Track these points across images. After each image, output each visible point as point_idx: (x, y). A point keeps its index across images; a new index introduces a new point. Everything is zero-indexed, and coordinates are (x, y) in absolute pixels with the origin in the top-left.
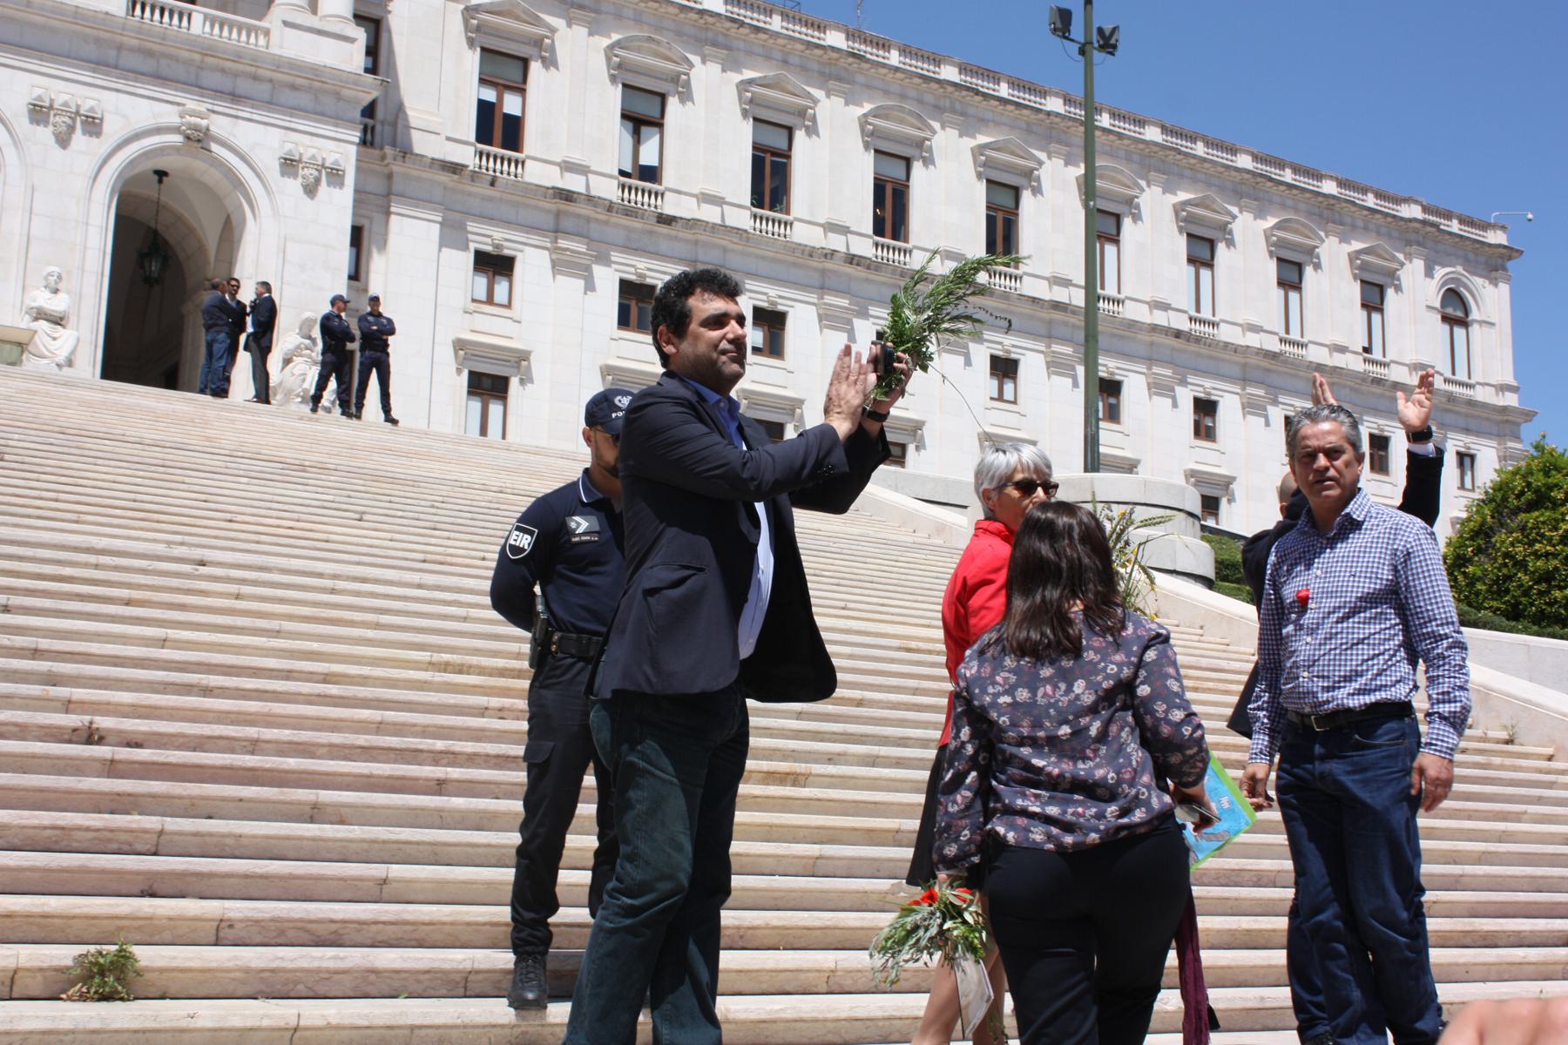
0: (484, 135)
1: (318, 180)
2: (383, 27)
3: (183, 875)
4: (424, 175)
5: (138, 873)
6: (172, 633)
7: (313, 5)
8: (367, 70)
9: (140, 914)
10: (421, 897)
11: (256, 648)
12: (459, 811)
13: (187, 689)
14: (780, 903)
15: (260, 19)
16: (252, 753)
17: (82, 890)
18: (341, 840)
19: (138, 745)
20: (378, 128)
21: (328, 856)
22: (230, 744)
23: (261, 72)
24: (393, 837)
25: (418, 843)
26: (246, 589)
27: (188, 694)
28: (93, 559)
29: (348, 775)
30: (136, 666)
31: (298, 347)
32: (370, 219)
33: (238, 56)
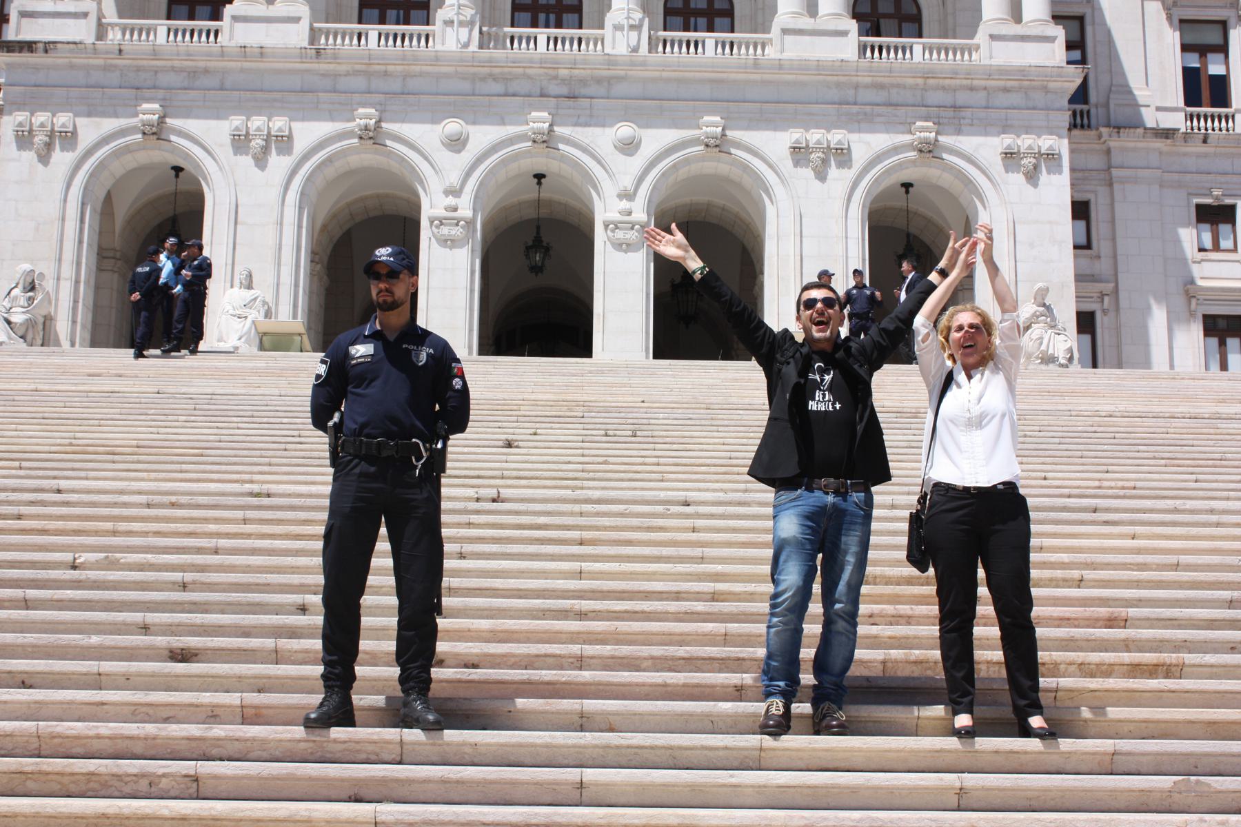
0: (1192, 96)
1: (1036, 167)
2: (1088, 20)
3: (384, 781)
4: (1140, 145)
5: (342, 780)
6: (586, 566)
7: (1016, 13)
8: (1069, 63)
9: (298, 818)
10: (623, 800)
11: (664, 574)
12: (728, 716)
13: (564, 614)
14: (1034, 804)
15: (972, 37)
16: (581, 669)
17: (293, 796)
18: (574, 746)
19: (475, 666)
20: (1093, 111)
21: (566, 762)
22: (558, 662)
23: (975, 82)
24: (623, 742)
25: (652, 748)
26: (700, 523)
27: (566, 618)
28: (577, 508)
29: (644, 685)
30: (538, 598)
31: (1035, 316)
32: (1095, 192)
33: (954, 74)
